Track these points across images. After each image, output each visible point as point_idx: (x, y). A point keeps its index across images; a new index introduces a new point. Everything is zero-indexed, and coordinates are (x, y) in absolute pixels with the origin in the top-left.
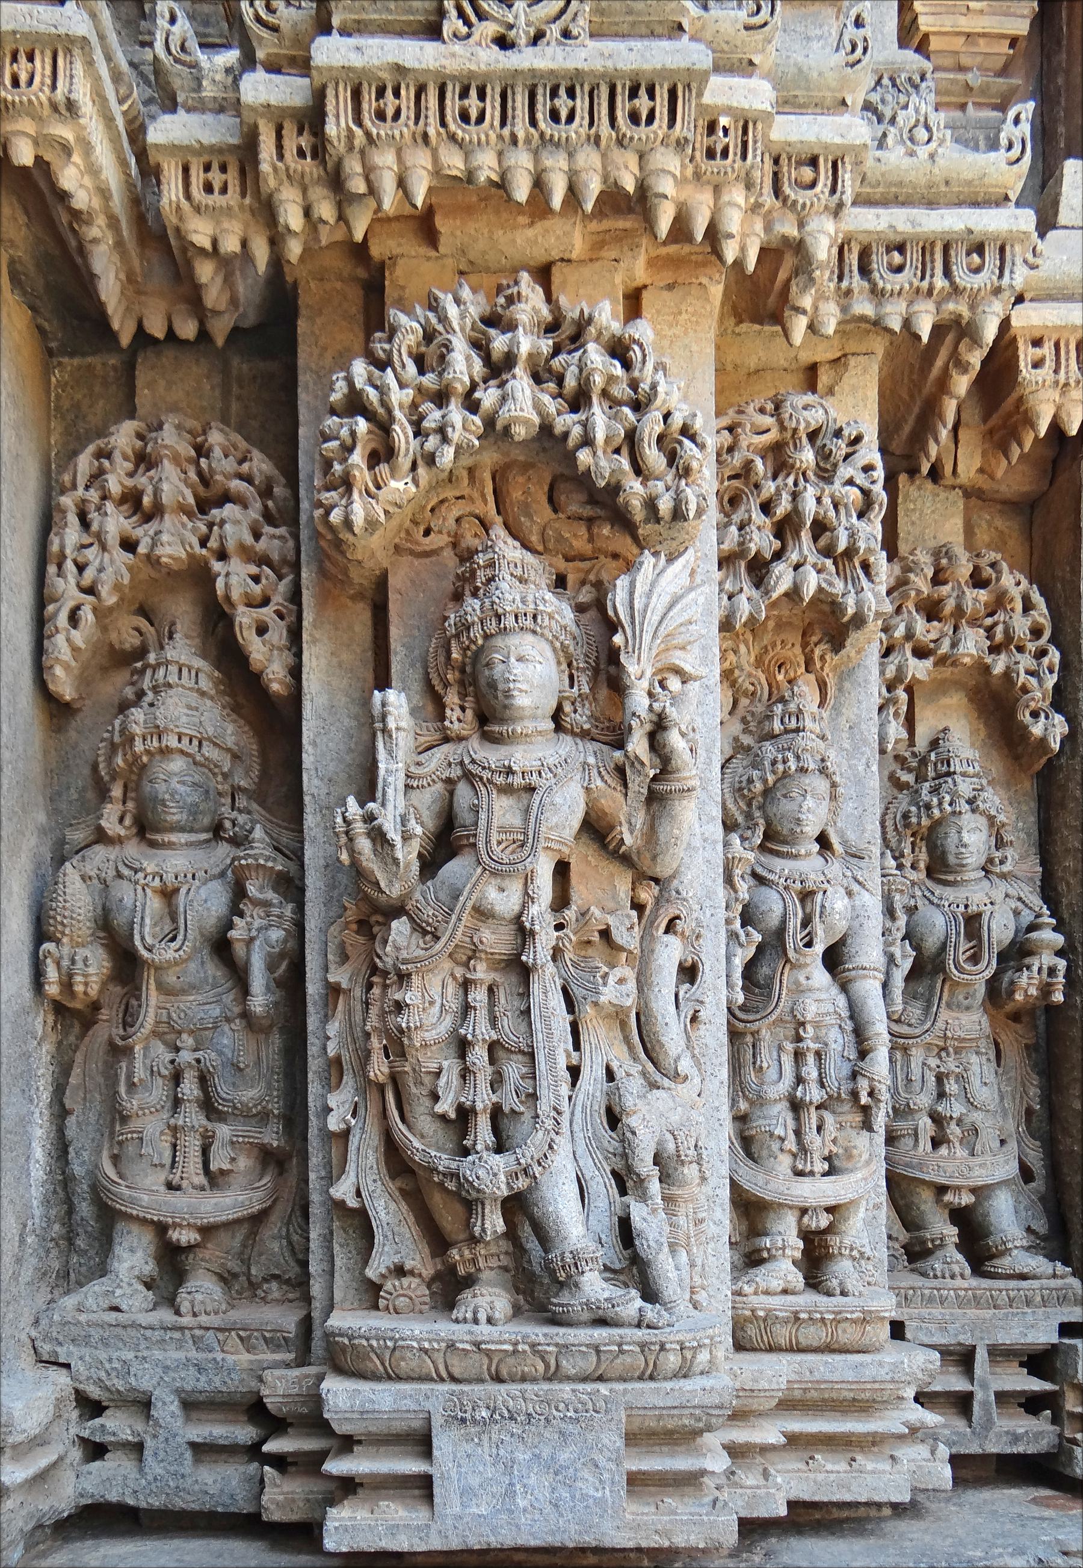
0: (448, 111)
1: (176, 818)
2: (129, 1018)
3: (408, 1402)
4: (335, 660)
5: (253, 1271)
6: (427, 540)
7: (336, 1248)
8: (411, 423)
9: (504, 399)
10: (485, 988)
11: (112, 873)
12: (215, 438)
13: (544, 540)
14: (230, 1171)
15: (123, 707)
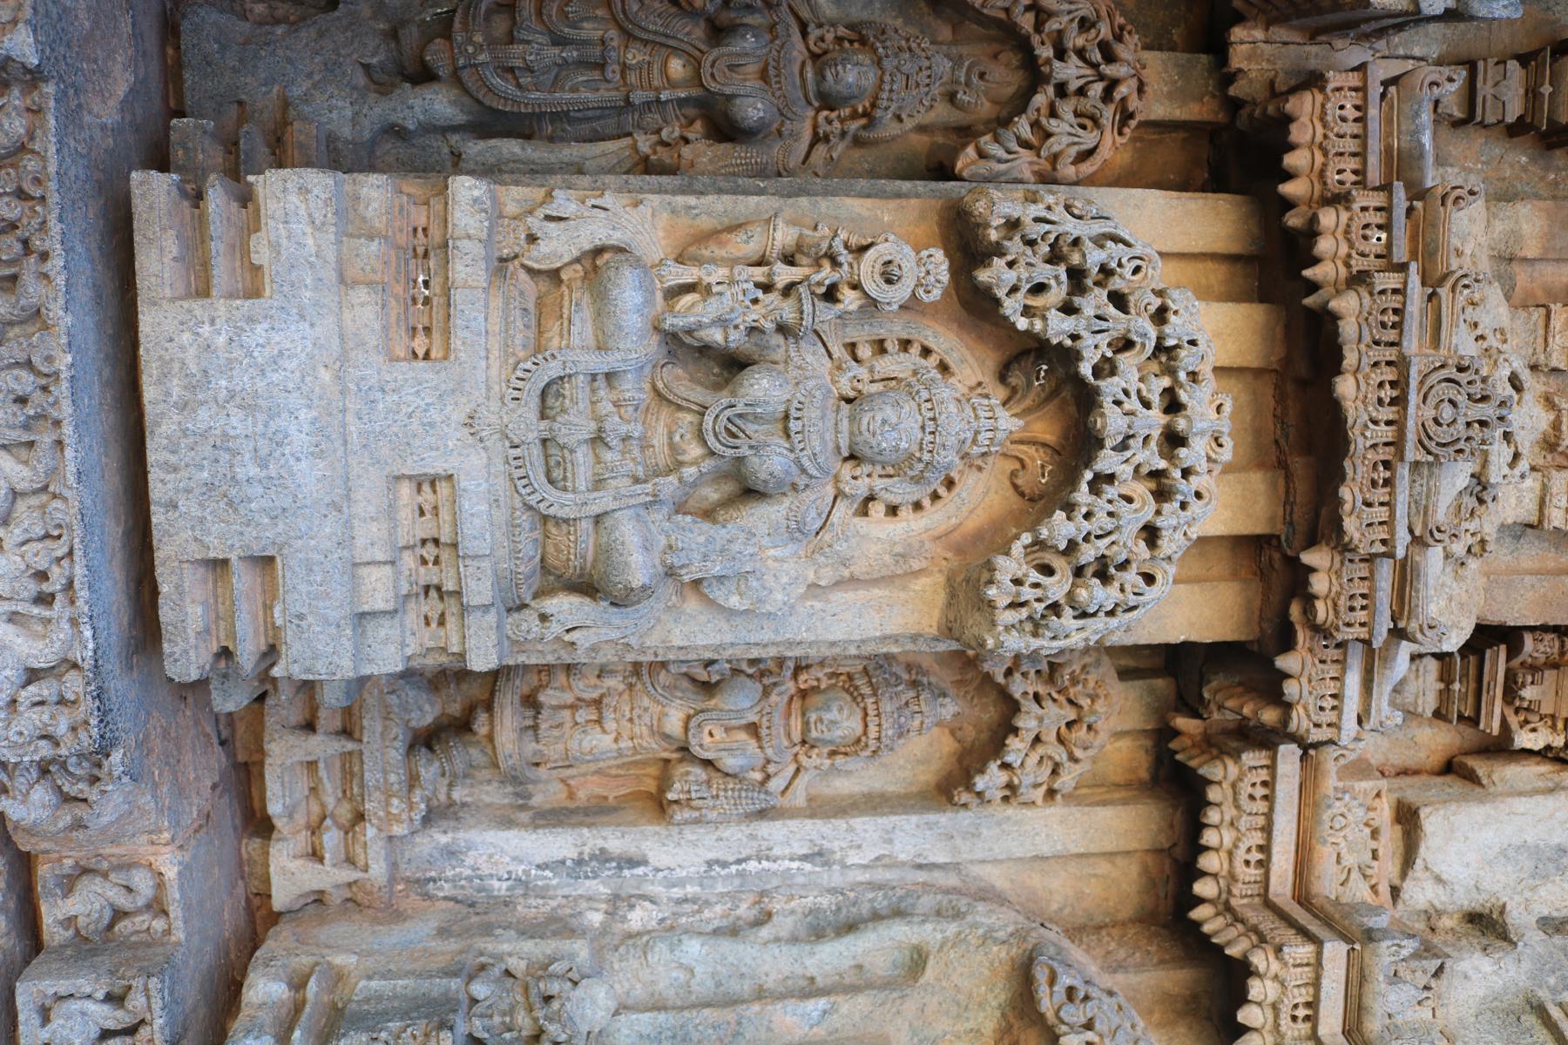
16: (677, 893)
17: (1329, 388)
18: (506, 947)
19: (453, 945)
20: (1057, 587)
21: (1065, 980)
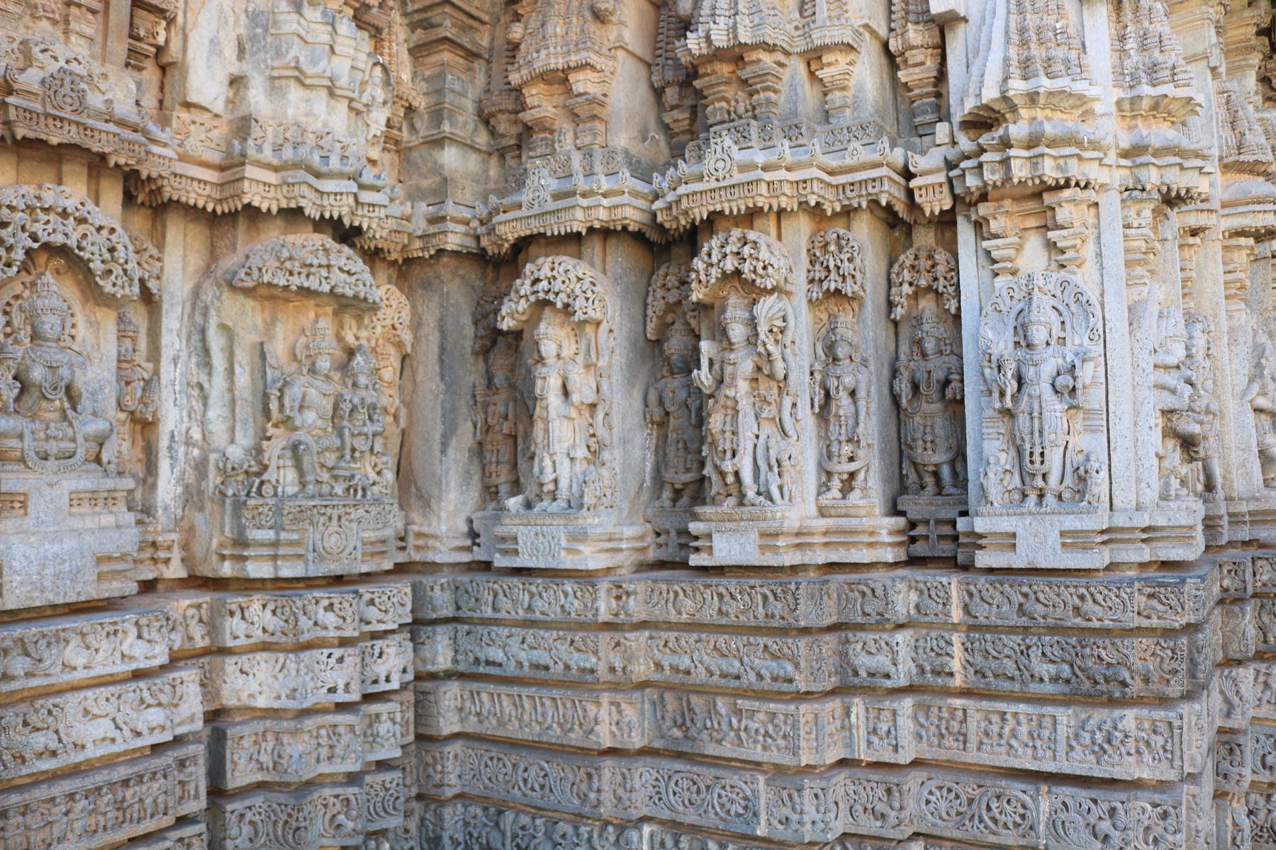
16: (186, 419)
17: (53, 147)
18: (211, 485)
19: (209, 505)
20: (117, 270)
21: (243, 275)
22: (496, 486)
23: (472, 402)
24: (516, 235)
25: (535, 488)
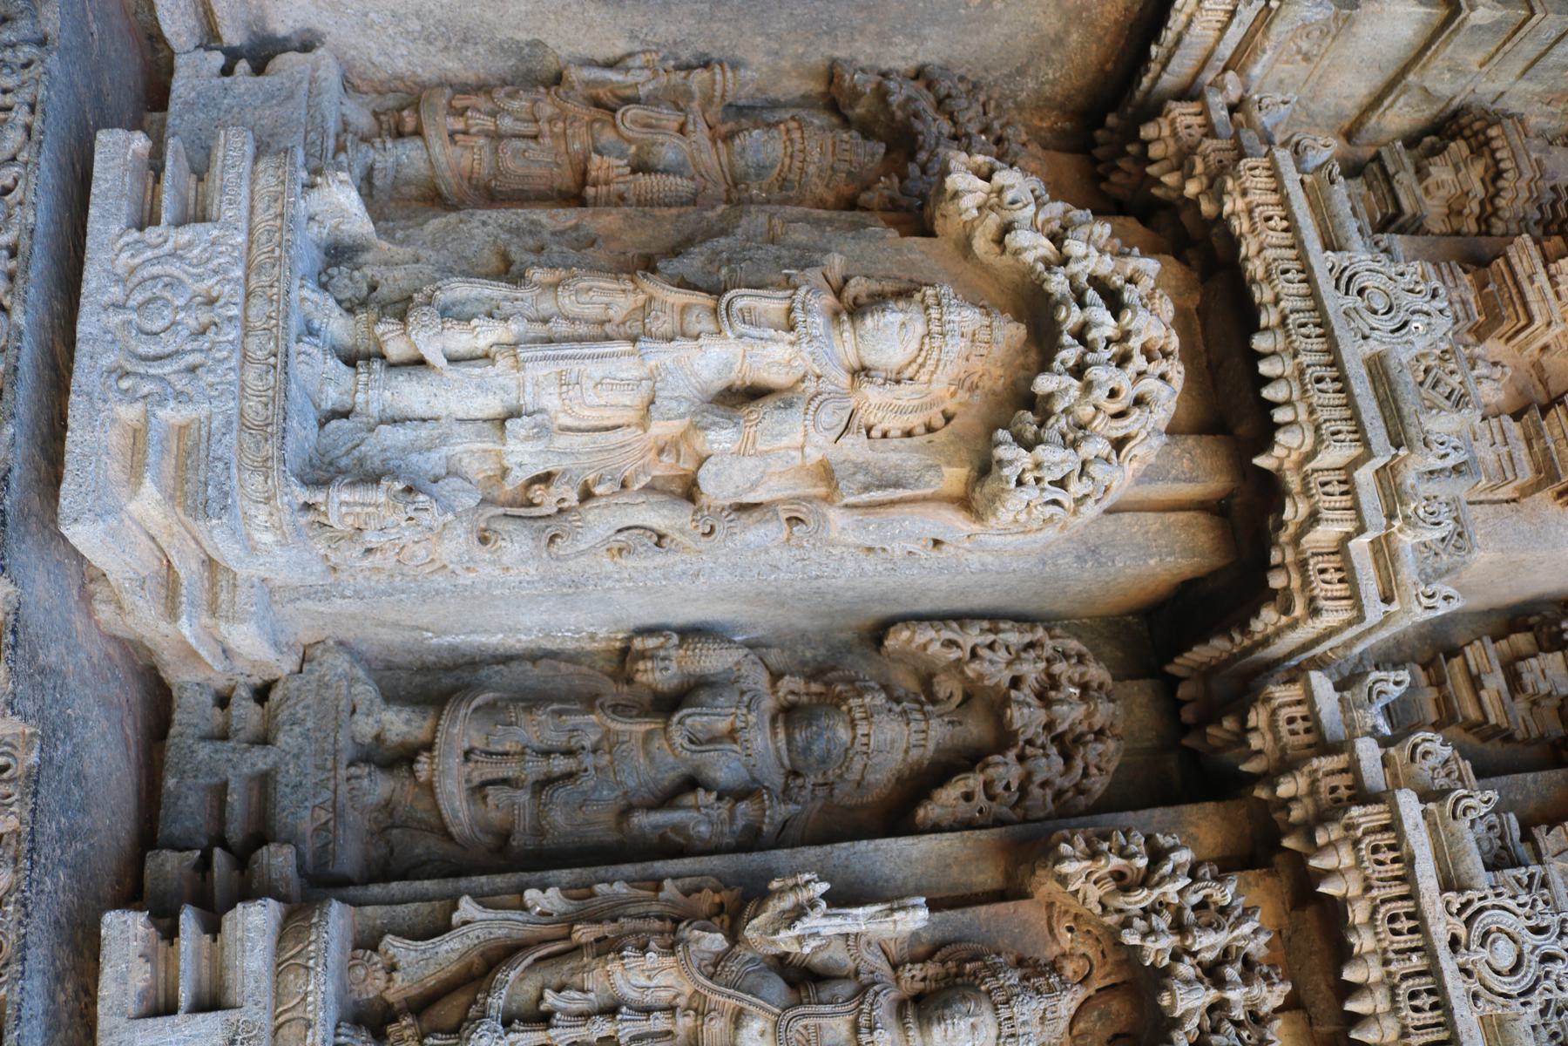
0: (1394, 905)
1: (797, 736)
2: (620, 709)
3: (253, 985)
4: (950, 861)
5: (395, 831)
6: (1063, 931)
7: (413, 906)
8: (1153, 903)
9: (1187, 982)
10: (669, 1027)
11: (744, 686)
12: (1111, 745)
13: (1082, 1035)
14: (485, 803)
15: (886, 688)
22: (418, 132)
23: (686, 55)
24: (1240, 225)
25: (394, 281)
